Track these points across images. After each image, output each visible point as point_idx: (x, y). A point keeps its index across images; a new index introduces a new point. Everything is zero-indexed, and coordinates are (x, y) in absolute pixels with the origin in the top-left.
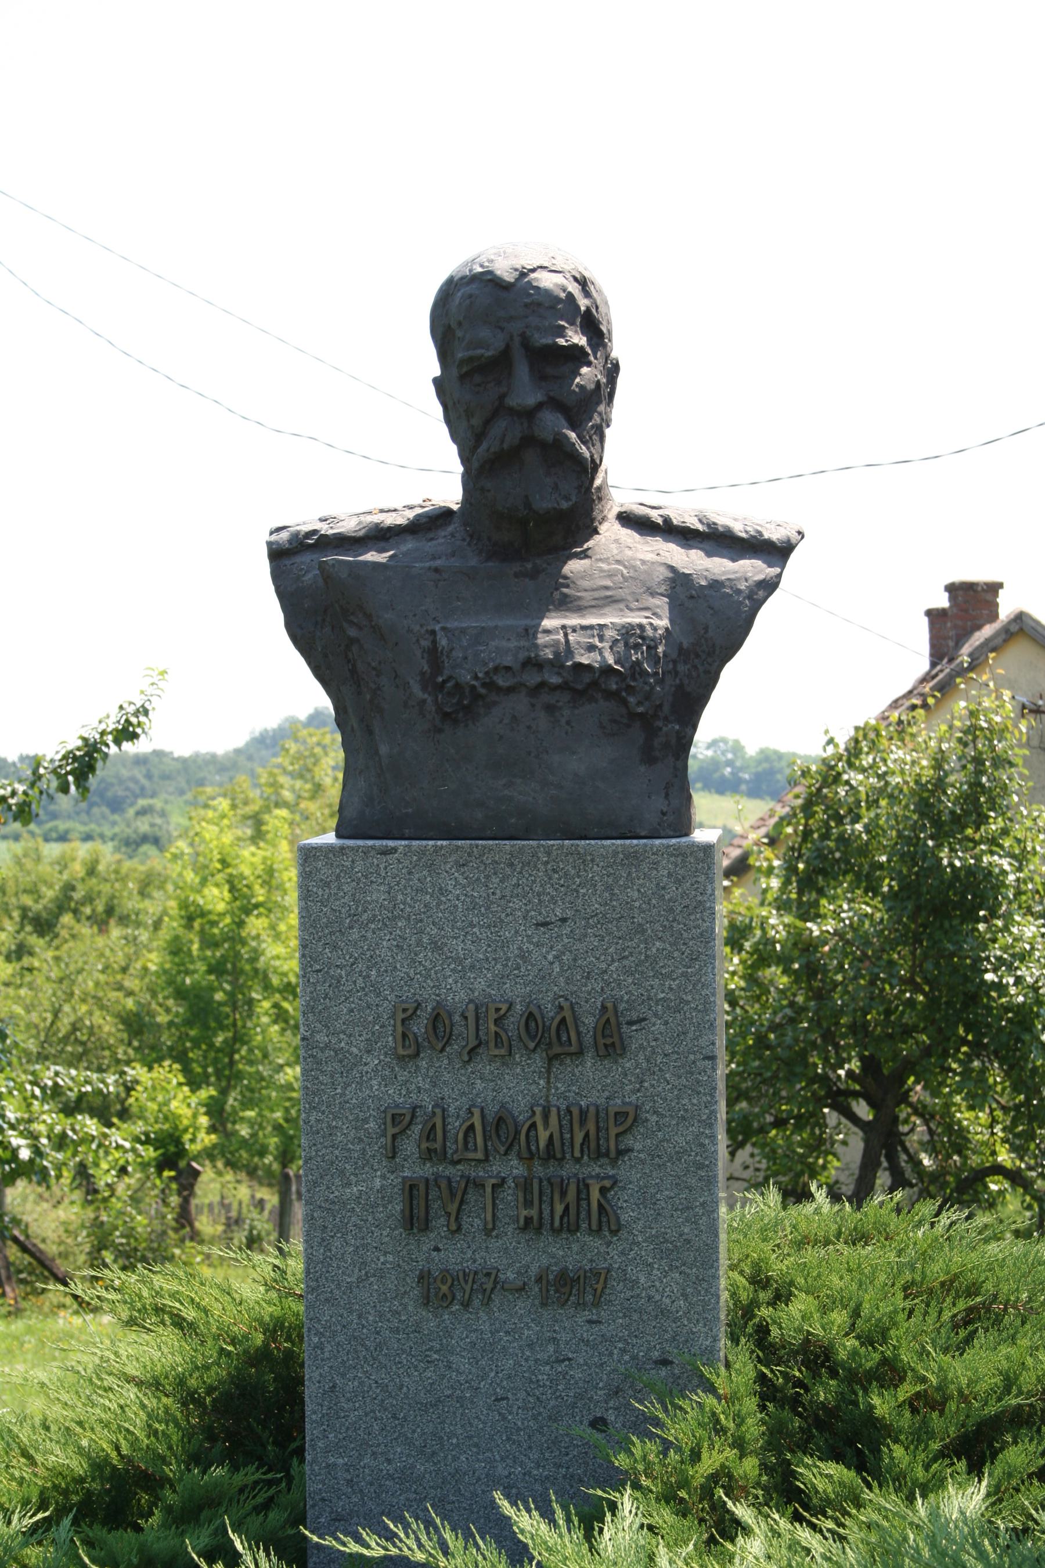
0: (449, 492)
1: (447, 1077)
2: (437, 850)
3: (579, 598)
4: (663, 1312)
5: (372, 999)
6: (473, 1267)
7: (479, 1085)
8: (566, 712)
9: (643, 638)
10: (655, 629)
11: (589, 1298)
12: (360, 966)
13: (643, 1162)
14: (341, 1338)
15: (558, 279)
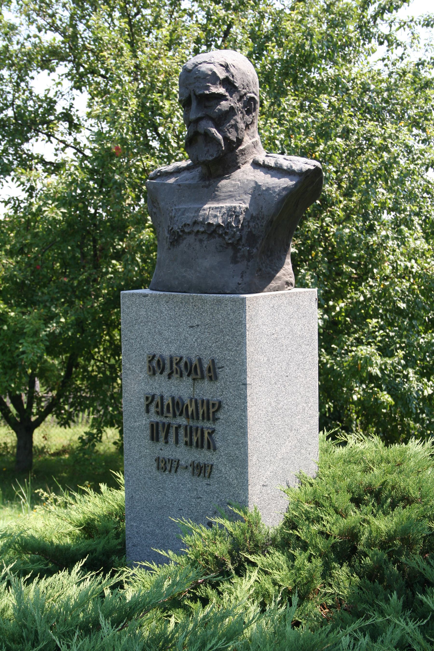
1: (164, 384)
2: (160, 295)
3: (220, 196)
4: (230, 484)
5: (141, 352)
6: (172, 458)
7: (173, 388)
8: (205, 242)
9: (234, 212)
10: (240, 208)
12: (138, 339)
13: (223, 424)
14: (134, 479)
15: (211, 66)
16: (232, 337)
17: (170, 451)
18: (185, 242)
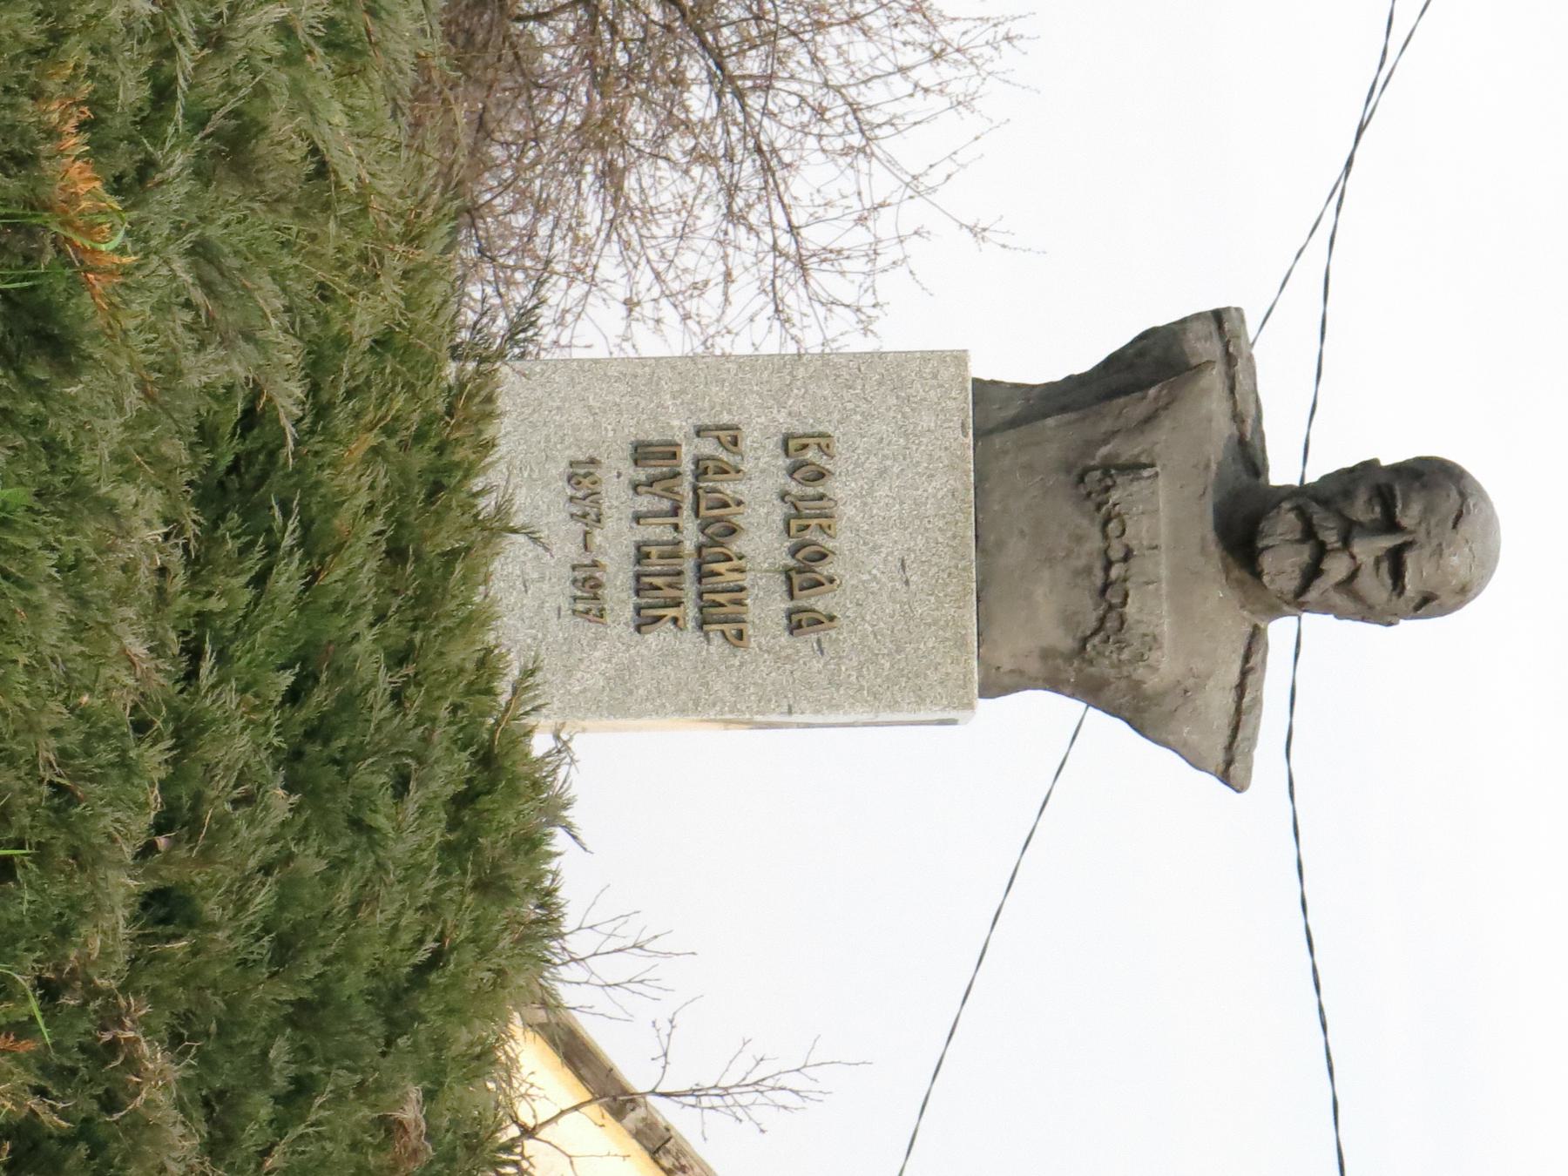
0: (1283, 471)
4: (569, 673)
5: (836, 416)
11: (580, 606)
12: (864, 406)
16: (888, 678)
17: (616, 496)
18: (1085, 522)
